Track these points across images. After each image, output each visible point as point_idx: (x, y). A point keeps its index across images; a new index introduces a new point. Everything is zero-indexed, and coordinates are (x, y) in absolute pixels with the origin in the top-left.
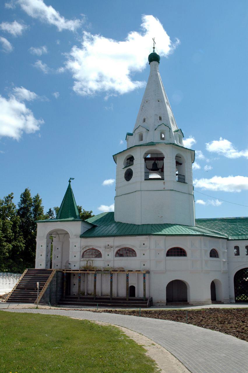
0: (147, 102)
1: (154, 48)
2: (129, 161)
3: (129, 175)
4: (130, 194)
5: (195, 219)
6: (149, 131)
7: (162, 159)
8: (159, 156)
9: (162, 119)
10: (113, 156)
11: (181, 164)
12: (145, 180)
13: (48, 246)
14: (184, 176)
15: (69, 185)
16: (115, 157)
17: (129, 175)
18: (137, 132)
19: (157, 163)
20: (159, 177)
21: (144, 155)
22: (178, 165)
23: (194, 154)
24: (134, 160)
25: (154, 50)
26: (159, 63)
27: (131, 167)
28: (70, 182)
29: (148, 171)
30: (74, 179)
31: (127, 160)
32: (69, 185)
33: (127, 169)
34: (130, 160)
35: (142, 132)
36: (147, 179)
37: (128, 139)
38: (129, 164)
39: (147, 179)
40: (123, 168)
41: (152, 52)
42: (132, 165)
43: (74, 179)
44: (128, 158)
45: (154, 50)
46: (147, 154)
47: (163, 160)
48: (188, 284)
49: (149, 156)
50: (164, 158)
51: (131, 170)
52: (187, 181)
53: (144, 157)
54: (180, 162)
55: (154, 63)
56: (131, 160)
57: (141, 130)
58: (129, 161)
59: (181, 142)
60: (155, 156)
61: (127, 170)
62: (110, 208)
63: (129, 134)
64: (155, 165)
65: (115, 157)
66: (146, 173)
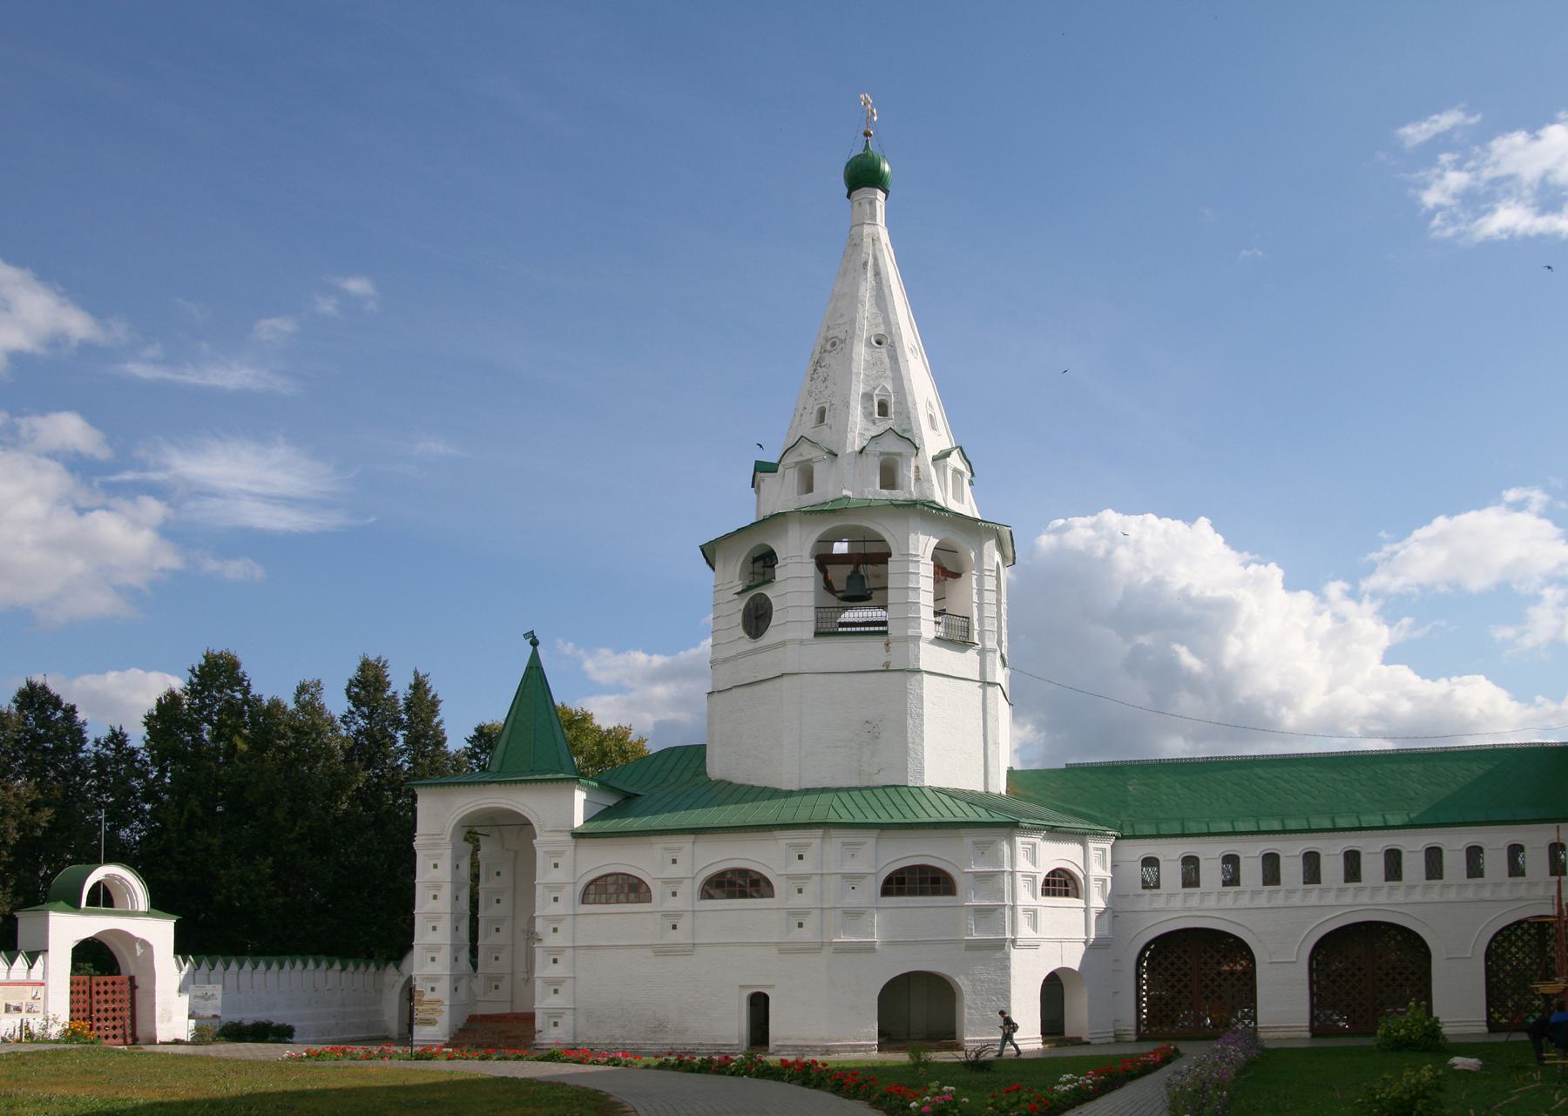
0: (834, 344)
3: (757, 618)
6: (837, 455)
7: (883, 558)
9: (892, 409)
12: (818, 634)
17: (757, 618)
18: (792, 458)
19: (862, 573)
21: (813, 546)
27: (770, 592)
29: (833, 601)
37: (759, 487)
38: (761, 578)
44: (755, 556)
46: (826, 540)
49: (841, 548)
50: (890, 555)
51: (767, 599)
53: (815, 554)
56: (764, 563)
57: (807, 452)
64: (856, 578)
66: (822, 610)
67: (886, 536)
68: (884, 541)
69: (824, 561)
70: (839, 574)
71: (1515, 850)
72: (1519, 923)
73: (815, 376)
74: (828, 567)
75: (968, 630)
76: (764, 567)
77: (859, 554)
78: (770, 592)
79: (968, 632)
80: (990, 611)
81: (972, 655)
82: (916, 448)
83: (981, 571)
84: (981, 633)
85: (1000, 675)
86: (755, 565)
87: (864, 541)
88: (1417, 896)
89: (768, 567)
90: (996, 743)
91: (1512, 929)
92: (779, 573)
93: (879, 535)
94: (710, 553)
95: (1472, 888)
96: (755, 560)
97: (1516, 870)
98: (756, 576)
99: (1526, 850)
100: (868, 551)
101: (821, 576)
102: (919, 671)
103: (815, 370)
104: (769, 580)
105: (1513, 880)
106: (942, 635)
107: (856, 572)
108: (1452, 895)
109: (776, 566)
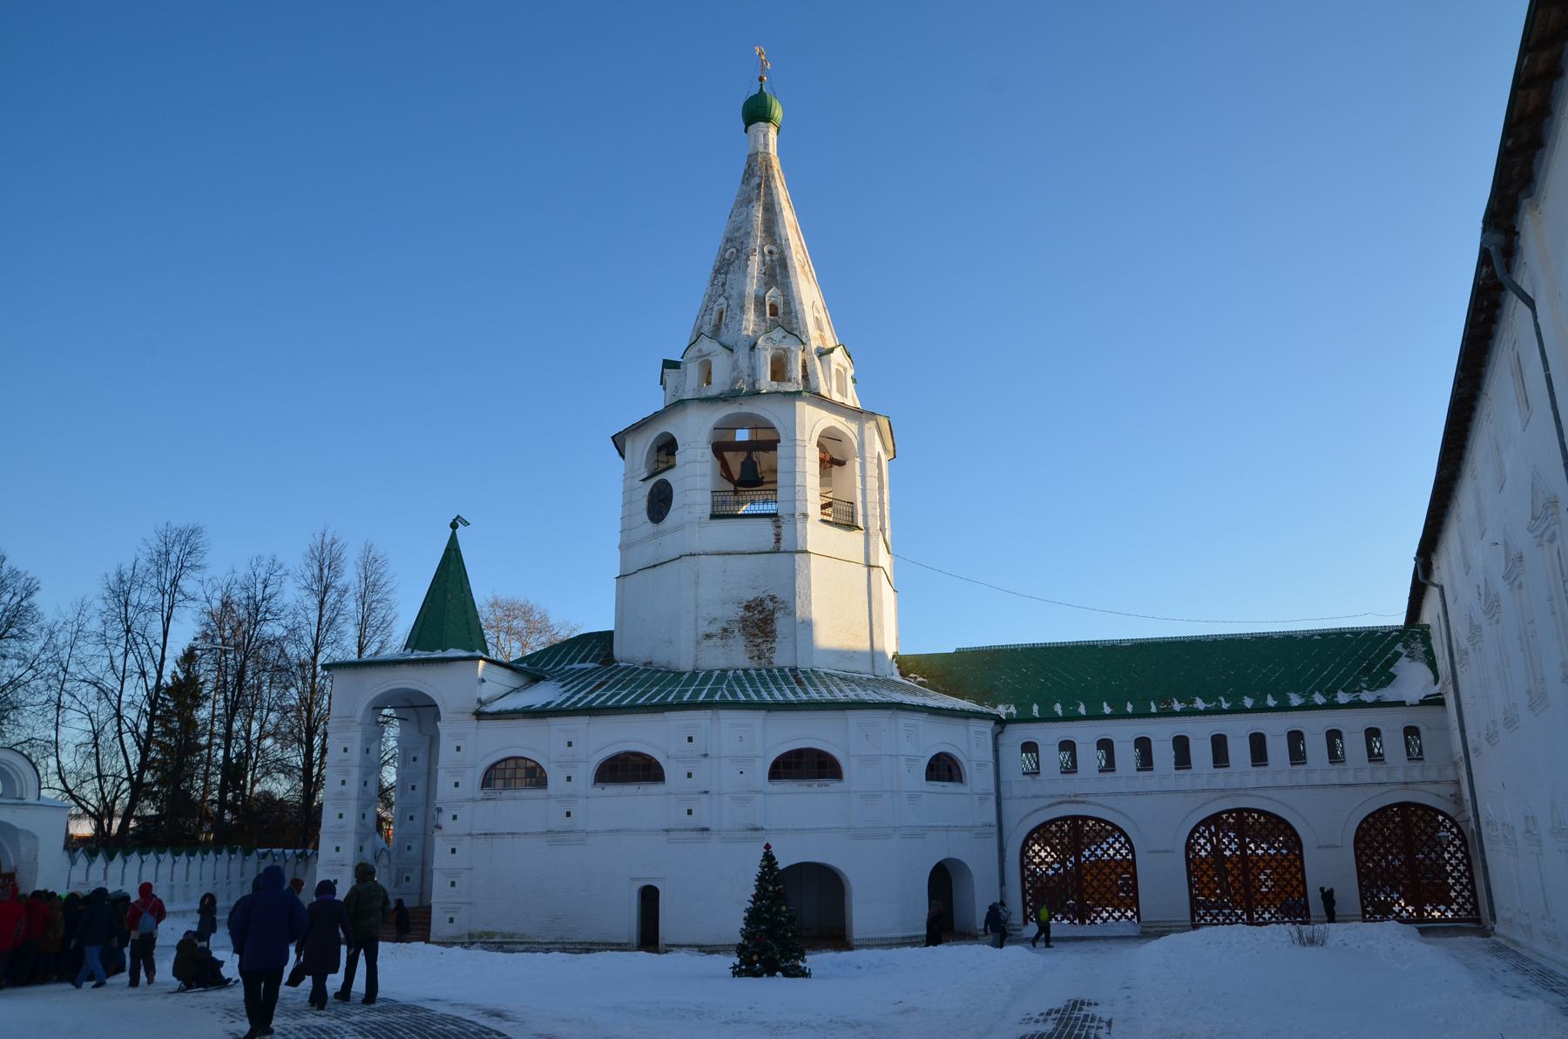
1: (761, 79)
2: (663, 453)
3: (660, 503)
4: (664, 565)
7: (772, 445)
8: (763, 436)
9: (781, 311)
10: (613, 438)
13: (368, 750)
14: (852, 503)
15: (453, 539)
16: (619, 441)
17: (660, 503)
19: (755, 459)
23: (888, 428)
24: (677, 449)
25: (761, 85)
27: (669, 476)
28: (454, 526)
31: (658, 452)
32: (453, 539)
33: (652, 483)
34: (668, 450)
35: (709, 354)
40: (644, 480)
42: (672, 467)
47: (776, 450)
48: (840, 871)
50: (779, 441)
53: (712, 441)
58: (663, 453)
61: (656, 485)
62: (601, 620)
63: (669, 365)
65: (619, 441)
66: (718, 494)
67: (775, 423)
68: (774, 428)
69: (719, 449)
70: (735, 461)
71: (1333, 736)
72: (1383, 810)
73: (716, 282)
75: (853, 515)
78: (669, 476)
79: (852, 516)
80: (873, 495)
81: (858, 536)
82: (803, 343)
83: (863, 458)
84: (865, 516)
85: (883, 559)
88: (1284, 780)
90: (881, 626)
91: (1377, 816)
92: (680, 457)
93: (769, 422)
95: (1335, 774)
97: (1334, 756)
99: (1345, 735)
100: (759, 438)
101: (718, 463)
102: (806, 552)
105: (1373, 765)
107: (749, 457)
108: (1316, 778)
109: (677, 452)
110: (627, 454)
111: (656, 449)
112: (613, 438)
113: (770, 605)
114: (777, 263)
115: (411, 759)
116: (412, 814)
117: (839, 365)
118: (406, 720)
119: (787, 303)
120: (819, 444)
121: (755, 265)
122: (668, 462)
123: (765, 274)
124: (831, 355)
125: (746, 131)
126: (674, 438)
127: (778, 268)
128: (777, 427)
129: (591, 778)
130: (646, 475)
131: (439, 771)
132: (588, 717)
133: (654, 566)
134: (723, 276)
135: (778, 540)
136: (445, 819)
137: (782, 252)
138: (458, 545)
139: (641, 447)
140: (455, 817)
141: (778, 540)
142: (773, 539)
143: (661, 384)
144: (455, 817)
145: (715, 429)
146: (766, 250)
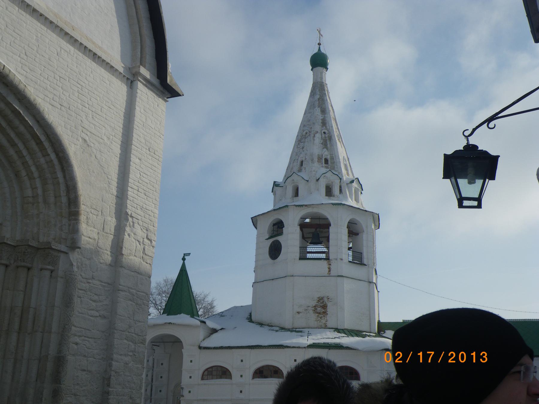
1: (319, 44)
2: (276, 226)
5: (379, 323)
8: (322, 222)
9: (329, 162)
10: (252, 218)
11: (357, 234)
14: (362, 253)
15: (184, 266)
20: (325, 250)
21: (299, 220)
22: (351, 235)
23: (378, 218)
25: (319, 47)
26: (327, 69)
27: (279, 238)
28: (184, 259)
30: (190, 254)
31: (273, 226)
32: (184, 266)
36: (303, 257)
37: (275, 192)
39: (303, 257)
40: (267, 239)
41: (316, 51)
43: (190, 254)
45: (319, 47)
46: (304, 218)
52: (365, 262)
53: (299, 223)
54: (354, 231)
55: (319, 69)
58: (276, 226)
59: (357, 200)
60: (317, 222)
61: (273, 242)
63: (276, 184)
65: (255, 221)
66: (302, 248)
73: (299, 146)
74: (303, 229)
76: (277, 228)
77: (317, 224)
86: (274, 227)
87: (320, 219)
89: (280, 228)
94: (255, 221)
96: (274, 225)
98: (274, 232)
103: (299, 144)
104: (281, 234)
106: (351, 260)
109: (284, 228)
110: (258, 227)
111: (272, 225)
112: (252, 218)
113: (326, 299)
114: (328, 139)
115: (161, 364)
116: (160, 389)
117: (356, 187)
118: (159, 346)
119: (332, 158)
120: (348, 227)
121: (318, 139)
122: (277, 231)
123: (322, 144)
124: (353, 184)
125: (312, 70)
126: (281, 220)
127: (328, 141)
128: (329, 218)
129: (251, 377)
130: (267, 237)
131: (183, 371)
132: (251, 349)
133: (273, 279)
134: (303, 143)
135: (330, 271)
136: (185, 392)
137: (329, 133)
138: (186, 269)
139: (266, 225)
140: (190, 392)
141: (330, 271)
142: (327, 270)
143: (272, 192)
144: (190, 392)
145: (301, 218)
146: (323, 132)
